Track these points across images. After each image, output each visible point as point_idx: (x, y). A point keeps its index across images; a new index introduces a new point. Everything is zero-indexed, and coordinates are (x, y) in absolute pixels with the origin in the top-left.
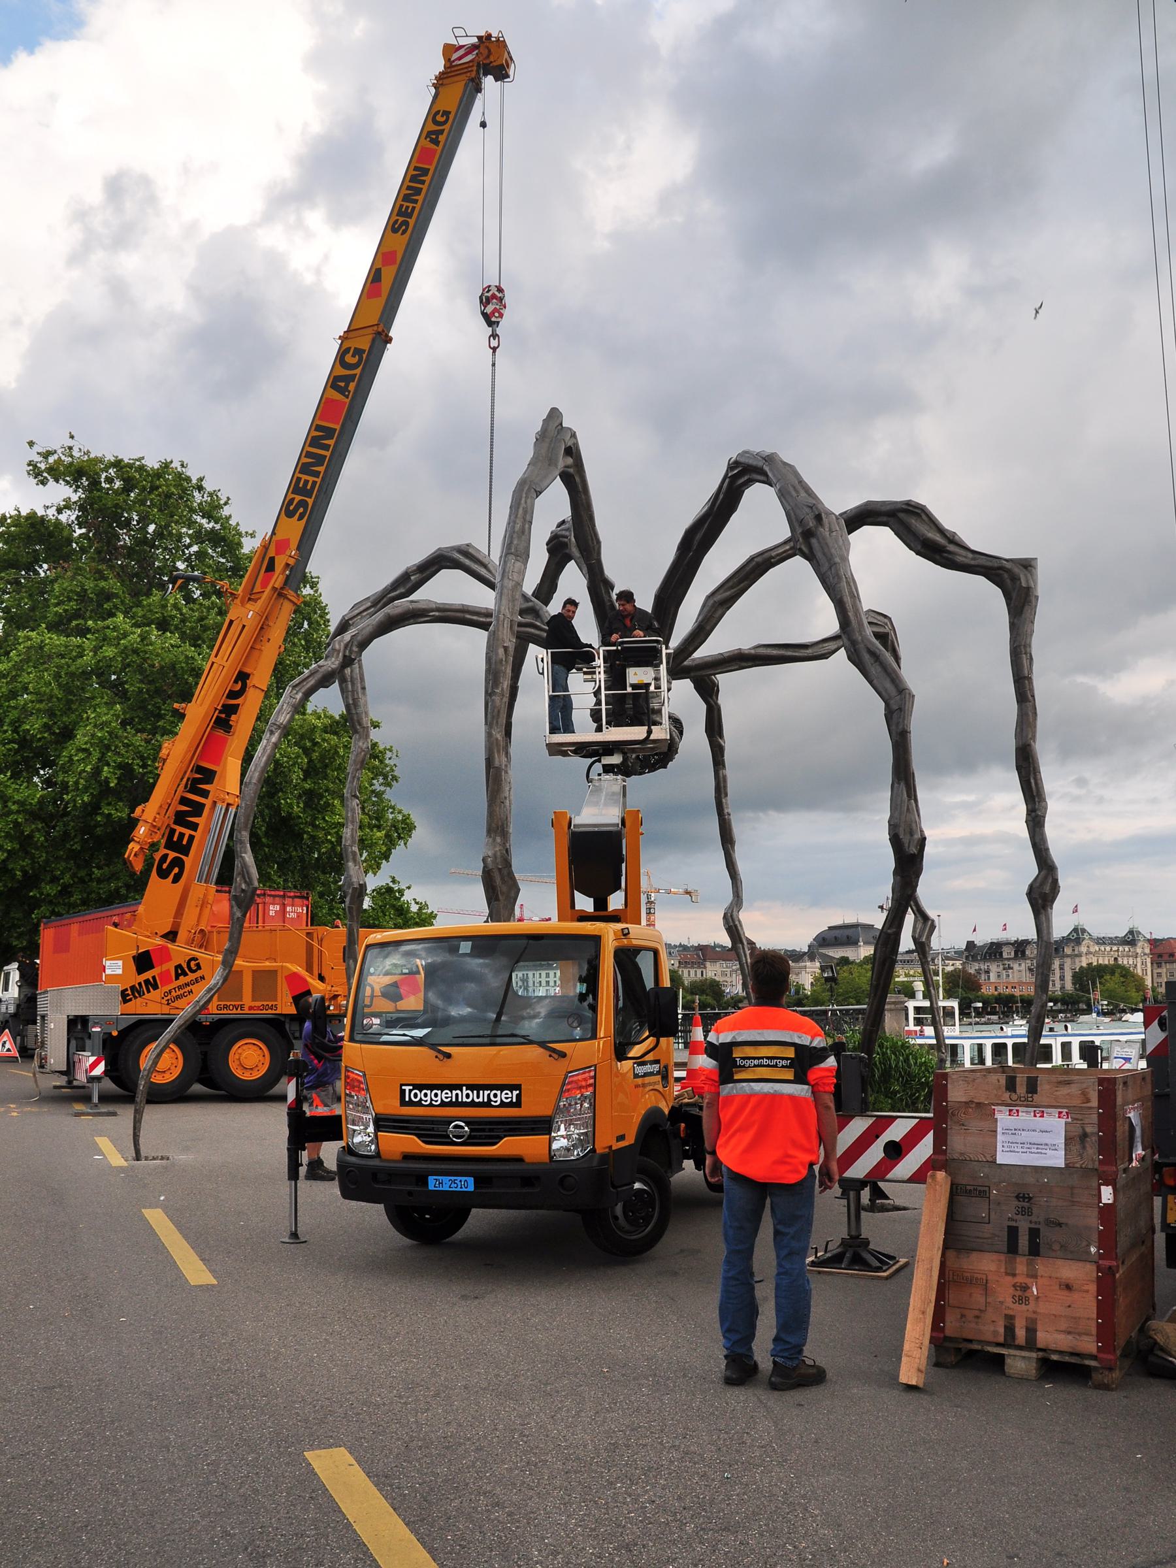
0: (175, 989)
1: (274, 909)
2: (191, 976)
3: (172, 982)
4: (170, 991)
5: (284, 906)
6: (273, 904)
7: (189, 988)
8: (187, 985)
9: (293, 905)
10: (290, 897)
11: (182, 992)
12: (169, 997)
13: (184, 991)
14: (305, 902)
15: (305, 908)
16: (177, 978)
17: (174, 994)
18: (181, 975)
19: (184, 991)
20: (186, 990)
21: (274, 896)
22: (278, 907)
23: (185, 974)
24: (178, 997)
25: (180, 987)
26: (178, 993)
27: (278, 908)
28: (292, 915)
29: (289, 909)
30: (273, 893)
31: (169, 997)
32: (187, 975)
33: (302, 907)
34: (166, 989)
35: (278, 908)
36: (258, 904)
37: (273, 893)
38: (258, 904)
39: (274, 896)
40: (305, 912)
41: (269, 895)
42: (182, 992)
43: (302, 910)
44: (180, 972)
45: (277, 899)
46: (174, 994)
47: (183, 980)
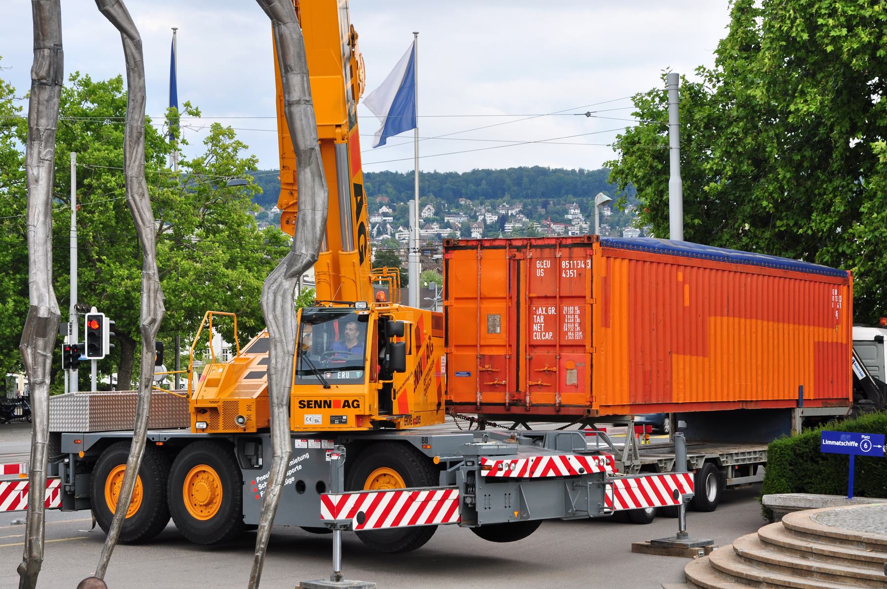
1: (542, 267)
5: (557, 262)
6: (541, 259)
9: (570, 258)
10: (566, 246)
14: (589, 251)
15: (589, 261)
22: (549, 262)
27: (548, 264)
28: (572, 273)
29: (564, 264)
33: (585, 258)
35: (548, 264)
36: (519, 261)
38: (519, 261)
40: (589, 267)
41: (532, 246)
43: (585, 264)
45: (547, 252)
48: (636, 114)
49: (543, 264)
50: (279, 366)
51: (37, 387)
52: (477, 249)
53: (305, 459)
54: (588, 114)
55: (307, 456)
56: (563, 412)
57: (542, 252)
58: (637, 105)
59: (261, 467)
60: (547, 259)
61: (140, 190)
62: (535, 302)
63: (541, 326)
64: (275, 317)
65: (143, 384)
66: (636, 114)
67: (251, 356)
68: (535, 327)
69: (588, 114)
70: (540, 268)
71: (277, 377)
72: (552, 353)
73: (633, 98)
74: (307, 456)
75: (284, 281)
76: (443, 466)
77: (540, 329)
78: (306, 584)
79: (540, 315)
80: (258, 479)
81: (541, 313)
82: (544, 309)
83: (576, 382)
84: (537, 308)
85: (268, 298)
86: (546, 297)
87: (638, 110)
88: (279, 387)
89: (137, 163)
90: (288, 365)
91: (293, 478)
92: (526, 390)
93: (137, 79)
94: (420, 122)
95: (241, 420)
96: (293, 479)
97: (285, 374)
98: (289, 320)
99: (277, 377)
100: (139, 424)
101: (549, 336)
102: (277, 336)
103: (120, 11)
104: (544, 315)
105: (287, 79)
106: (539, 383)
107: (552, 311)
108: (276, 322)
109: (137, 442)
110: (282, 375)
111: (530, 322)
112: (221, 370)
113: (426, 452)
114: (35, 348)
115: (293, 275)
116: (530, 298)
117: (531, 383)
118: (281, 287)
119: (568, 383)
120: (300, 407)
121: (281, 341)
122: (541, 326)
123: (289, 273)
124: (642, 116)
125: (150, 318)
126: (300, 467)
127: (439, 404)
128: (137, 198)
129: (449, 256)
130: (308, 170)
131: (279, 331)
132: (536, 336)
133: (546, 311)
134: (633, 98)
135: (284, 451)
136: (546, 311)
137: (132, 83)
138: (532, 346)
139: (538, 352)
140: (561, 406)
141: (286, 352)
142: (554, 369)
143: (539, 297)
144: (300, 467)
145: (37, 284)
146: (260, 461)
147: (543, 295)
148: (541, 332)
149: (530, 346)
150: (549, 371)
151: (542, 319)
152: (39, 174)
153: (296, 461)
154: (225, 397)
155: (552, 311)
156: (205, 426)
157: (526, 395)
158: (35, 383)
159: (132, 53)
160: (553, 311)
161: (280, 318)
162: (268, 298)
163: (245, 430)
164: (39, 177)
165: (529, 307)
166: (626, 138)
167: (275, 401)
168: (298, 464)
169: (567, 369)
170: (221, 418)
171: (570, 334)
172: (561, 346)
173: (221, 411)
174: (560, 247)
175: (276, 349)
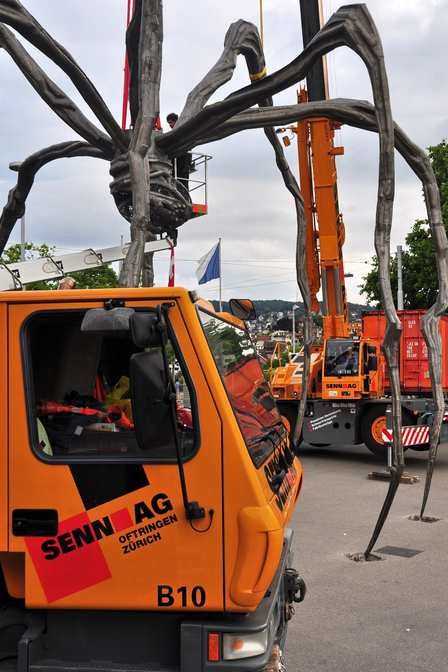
0: (134, 532)
2: (159, 517)
3: (132, 525)
4: (128, 536)
6: (411, 320)
7: (154, 532)
8: (152, 527)
11: (145, 536)
12: (127, 543)
13: (148, 535)
16: (139, 520)
17: (133, 539)
18: (144, 516)
19: (148, 535)
20: (151, 534)
21: (411, 315)
23: (150, 516)
24: (139, 543)
25: (141, 531)
26: (140, 538)
27: (414, 322)
30: (410, 312)
31: (127, 543)
32: (153, 516)
34: (124, 533)
35: (414, 322)
37: (410, 312)
39: (411, 315)
41: (406, 314)
42: (145, 536)
44: (142, 512)
45: (414, 317)
46: (133, 539)
47: (146, 522)
48: (373, 265)
49: (412, 322)
50: (437, 362)
51: (394, 369)
52: (378, 316)
53: (339, 412)
54: (366, 262)
55: (340, 411)
56: (423, 390)
57: (411, 317)
58: (374, 261)
59: (312, 416)
60: (414, 320)
61: (305, 277)
62: (407, 340)
63: (411, 351)
64: (432, 337)
65: (306, 374)
66: (373, 265)
67: (296, 364)
68: (408, 352)
69: (366, 262)
70: (410, 324)
71: (436, 368)
72: (416, 363)
73: (373, 258)
74: (340, 411)
75: (434, 318)
76: (418, 415)
77: (411, 352)
78: (376, 473)
79: (410, 346)
80: (311, 422)
81: (411, 346)
82: (412, 343)
83: (428, 377)
84: (409, 343)
85: (427, 327)
86: (413, 338)
87: (375, 263)
88: (437, 373)
89: (303, 263)
90: (441, 362)
91: (331, 422)
92: (404, 381)
93: (303, 221)
94: (222, 275)
95: (295, 394)
96: (331, 422)
97: (439, 366)
98: (438, 338)
99: (436, 368)
100: (304, 394)
101: (415, 356)
102: (434, 346)
103: (296, 187)
104: (412, 346)
105: (432, 212)
106: (410, 377)
107: (416, 344)
108: (433, 339)
109: (303, 403)
110: (438, 367)
111: (405, 349)
112: (284, 370)
113: (409, 409)
114: (393, 347)
115: (438, 315)
116: (405, 338)
117: (406, 377)
118: (433, 321)
119: (425, 377)
120: (327, 387)
121: (437, 349)
122: (411, 351)
123: (436, 314)
124: (376, 265)
125: (310, 341)
126: (336, 416)
127: (382, 387)
128: (303, 280)
129: (363, 319)
130: (444, 260)
131: (435, 344)
132: (408, 356)
133: (414, 344)
134: (373, 258)
135: (442, 407)
136: (414, 344)
137: (300, 223)
138: (407, 360)
139: (409, 363)
140: (421, 388)
141: (439, 355)
142: (418, 371)
143: (409, 338)
144: (336, 416)
145: (392, 311)
146: (312, 413)
147: (412, 337)
148: (411, 354)
149: (405, 360)
150: (415, 372)
151: (411, 348)
152: (384, 249)
153: (333, 413)
154: (287, 382)
155: (416, 344)
156: (278, 396)
157: (403, 383)
158: (393, 367)
159: (301, 209)
160: (417, 344)
161: (435, 337)
162: (427, 327)
163: (297, 398)
164: (384, 252)
165: (405, 342)
166: (371, 274)
167: (436, 380)
168: (335, 415)
169: (424, 371)
170: (286, 393)
171: (425, 354)
172: (421, 360)
173: (286, 389)
174: (421, 314)
175: (434, 354)
